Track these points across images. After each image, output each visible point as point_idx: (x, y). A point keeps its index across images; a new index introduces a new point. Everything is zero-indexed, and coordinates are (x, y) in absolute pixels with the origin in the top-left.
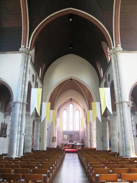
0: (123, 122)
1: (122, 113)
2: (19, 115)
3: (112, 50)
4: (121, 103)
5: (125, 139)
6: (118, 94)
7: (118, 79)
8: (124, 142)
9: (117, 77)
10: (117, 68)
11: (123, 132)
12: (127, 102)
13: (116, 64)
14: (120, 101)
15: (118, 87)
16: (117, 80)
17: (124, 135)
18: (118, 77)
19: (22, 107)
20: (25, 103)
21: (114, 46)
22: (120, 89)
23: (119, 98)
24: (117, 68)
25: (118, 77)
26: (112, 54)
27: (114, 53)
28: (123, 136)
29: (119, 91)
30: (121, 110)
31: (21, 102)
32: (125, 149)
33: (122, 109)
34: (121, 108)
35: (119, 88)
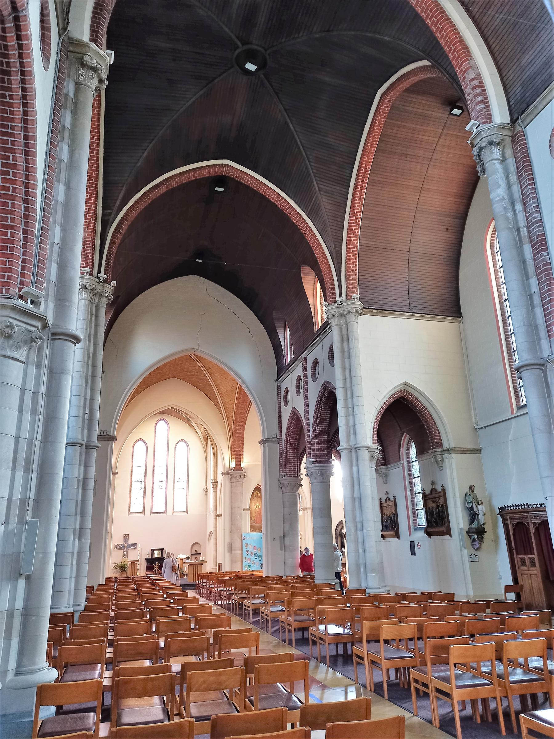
0: (360, 499)
1: (355, 475)
2: (78, 480)
3: (335, 305)
4: (353, 451)
5: (363, 543)
6: (347, 426)
7: (348, 385)
8: (361, 551)
9: (345, 379)
10: (346, 355)
11: (359, 525)
12: (368, 448)
13: (345, 344)
14: (352, 443)
15: (347, 407)
16: (345, 388)
17: (359, 533)
18: (348, 380)
19: (85, 458)
20: (94, 444)
21: (341, 296)
22: (352, 413)
23: (348, 436)
24: (346, 355)
25: (348, 380)
26: (336, 316)
27: (342, 315)
28: (356, 535)
29: (351, 418)
30: (355, 468)
31: (84, 443)
32: (362, 570)
33: (358, 465)
34: (354, 462)
35: (350, 409)
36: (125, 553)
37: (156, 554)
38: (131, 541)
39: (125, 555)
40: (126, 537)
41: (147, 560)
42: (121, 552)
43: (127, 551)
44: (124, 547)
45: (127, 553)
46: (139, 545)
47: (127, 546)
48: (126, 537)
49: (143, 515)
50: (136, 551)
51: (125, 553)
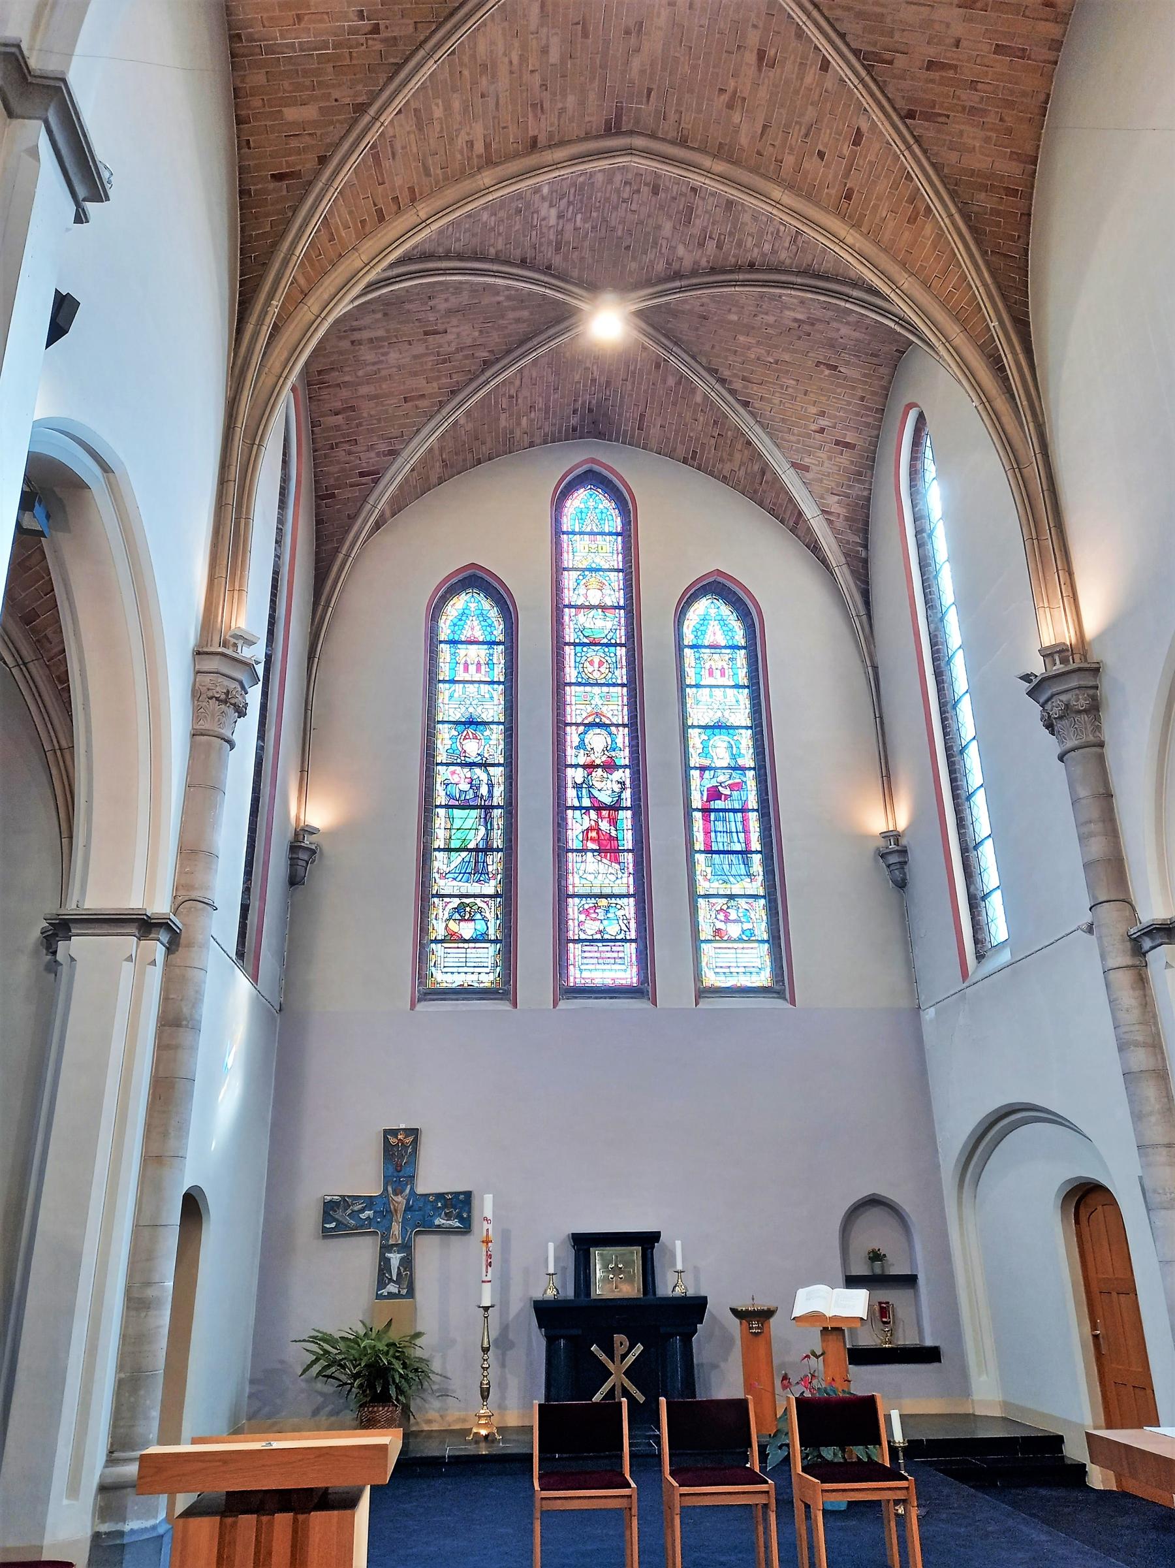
36: (395, 1258)
37: (611, 1281)
38: (434, 1176)
39: (396, 1281)
40: (400, 1151)
41: (545, 1312)
42: (359, 1255)
43: (406, 1247)
44: (386, 1214)
45: (407, 1263)
46: (486, 1206)
47: (405, 1211)
48: (400, 1151)
49: (504, 1006)
50: (473, 1242)
51: (395, 1258)
